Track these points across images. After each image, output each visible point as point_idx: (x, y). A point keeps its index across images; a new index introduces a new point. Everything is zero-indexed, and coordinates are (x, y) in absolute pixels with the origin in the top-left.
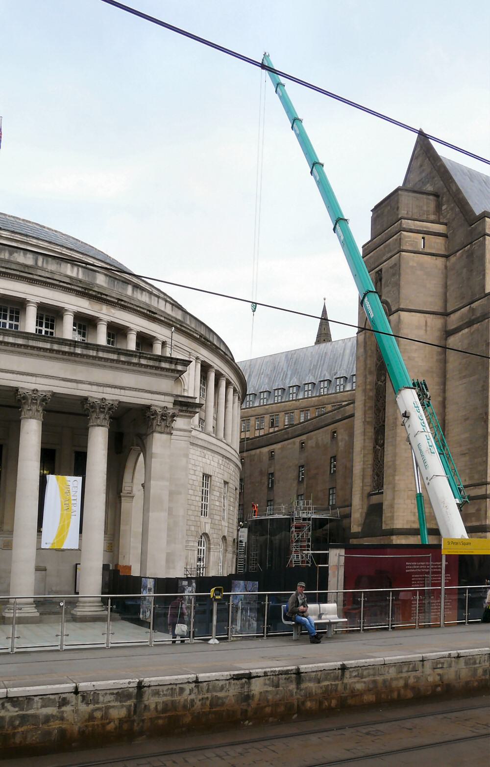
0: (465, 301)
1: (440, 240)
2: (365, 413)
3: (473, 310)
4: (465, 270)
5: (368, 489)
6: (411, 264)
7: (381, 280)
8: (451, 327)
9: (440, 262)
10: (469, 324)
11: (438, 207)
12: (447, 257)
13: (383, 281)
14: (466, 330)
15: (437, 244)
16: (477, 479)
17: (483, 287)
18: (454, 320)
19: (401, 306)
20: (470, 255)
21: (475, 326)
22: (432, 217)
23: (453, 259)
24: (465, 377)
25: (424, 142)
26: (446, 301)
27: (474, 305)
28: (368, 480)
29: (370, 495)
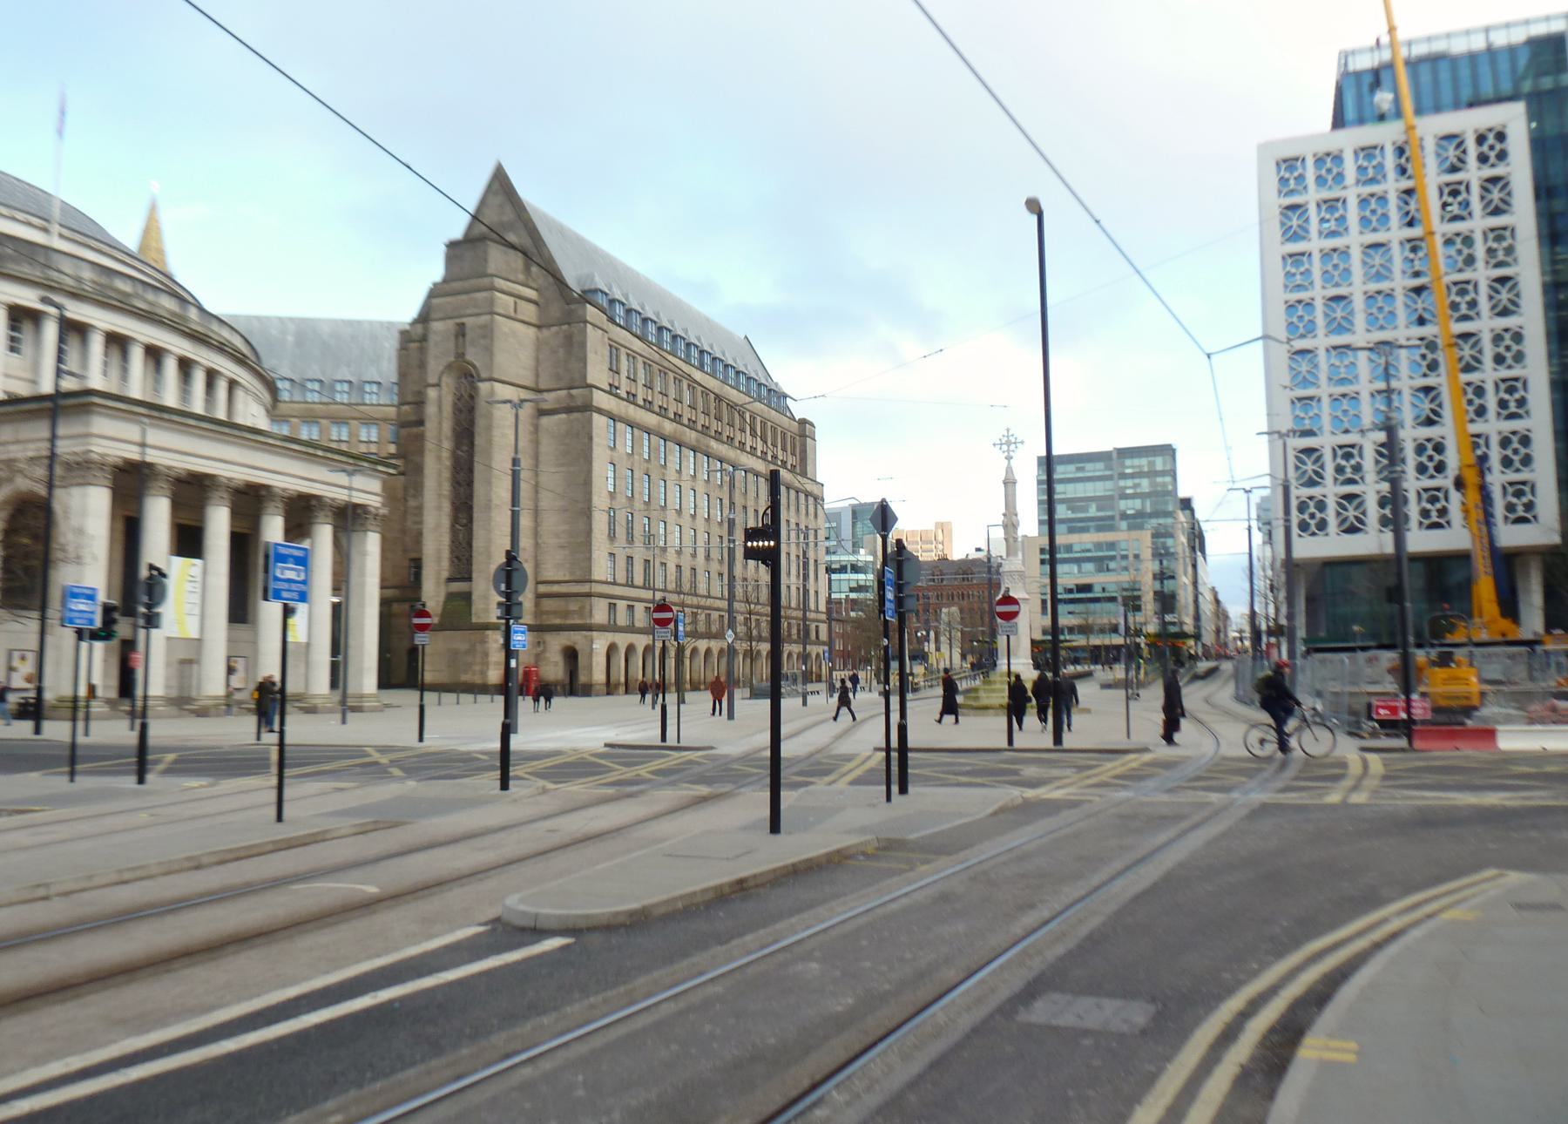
0: (562, 384)
1: (532, 307)
2: (440, 485)
3: (571, 396)
4: (561, 352)
5: (445, 574)
6: (506, 330)
7: (464, 335)
8: (545, 406)
9: (532, 331)
10: (569, 410)
11: (527, 269)
12: (539, 327)
13: (468, 338)
14: (564, 416)
15: (529, 312)
16: (578, 575)
17: (585, 377)
18: (550, 400)
19: (496, 376)
20: (569, 339)
21: (576, 415)
22: (521, 277)
23: (546, 333)
24: (562, 465)
25: (500, 184)
26: (537, 376)
27: (574, 392)
28: (446, 563)
29: (450, 580)
